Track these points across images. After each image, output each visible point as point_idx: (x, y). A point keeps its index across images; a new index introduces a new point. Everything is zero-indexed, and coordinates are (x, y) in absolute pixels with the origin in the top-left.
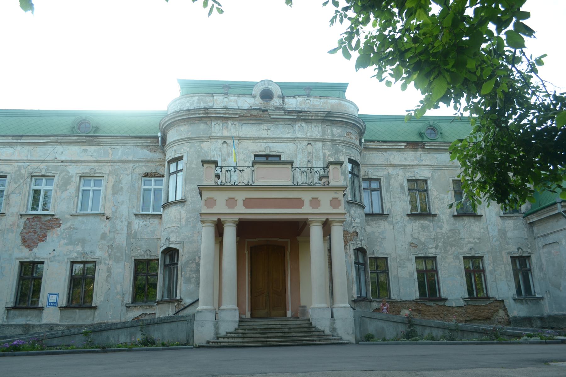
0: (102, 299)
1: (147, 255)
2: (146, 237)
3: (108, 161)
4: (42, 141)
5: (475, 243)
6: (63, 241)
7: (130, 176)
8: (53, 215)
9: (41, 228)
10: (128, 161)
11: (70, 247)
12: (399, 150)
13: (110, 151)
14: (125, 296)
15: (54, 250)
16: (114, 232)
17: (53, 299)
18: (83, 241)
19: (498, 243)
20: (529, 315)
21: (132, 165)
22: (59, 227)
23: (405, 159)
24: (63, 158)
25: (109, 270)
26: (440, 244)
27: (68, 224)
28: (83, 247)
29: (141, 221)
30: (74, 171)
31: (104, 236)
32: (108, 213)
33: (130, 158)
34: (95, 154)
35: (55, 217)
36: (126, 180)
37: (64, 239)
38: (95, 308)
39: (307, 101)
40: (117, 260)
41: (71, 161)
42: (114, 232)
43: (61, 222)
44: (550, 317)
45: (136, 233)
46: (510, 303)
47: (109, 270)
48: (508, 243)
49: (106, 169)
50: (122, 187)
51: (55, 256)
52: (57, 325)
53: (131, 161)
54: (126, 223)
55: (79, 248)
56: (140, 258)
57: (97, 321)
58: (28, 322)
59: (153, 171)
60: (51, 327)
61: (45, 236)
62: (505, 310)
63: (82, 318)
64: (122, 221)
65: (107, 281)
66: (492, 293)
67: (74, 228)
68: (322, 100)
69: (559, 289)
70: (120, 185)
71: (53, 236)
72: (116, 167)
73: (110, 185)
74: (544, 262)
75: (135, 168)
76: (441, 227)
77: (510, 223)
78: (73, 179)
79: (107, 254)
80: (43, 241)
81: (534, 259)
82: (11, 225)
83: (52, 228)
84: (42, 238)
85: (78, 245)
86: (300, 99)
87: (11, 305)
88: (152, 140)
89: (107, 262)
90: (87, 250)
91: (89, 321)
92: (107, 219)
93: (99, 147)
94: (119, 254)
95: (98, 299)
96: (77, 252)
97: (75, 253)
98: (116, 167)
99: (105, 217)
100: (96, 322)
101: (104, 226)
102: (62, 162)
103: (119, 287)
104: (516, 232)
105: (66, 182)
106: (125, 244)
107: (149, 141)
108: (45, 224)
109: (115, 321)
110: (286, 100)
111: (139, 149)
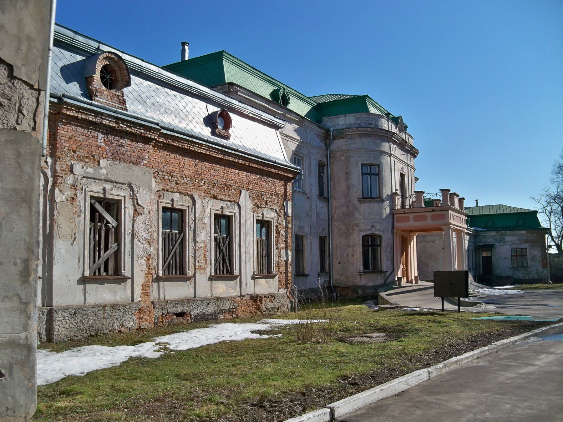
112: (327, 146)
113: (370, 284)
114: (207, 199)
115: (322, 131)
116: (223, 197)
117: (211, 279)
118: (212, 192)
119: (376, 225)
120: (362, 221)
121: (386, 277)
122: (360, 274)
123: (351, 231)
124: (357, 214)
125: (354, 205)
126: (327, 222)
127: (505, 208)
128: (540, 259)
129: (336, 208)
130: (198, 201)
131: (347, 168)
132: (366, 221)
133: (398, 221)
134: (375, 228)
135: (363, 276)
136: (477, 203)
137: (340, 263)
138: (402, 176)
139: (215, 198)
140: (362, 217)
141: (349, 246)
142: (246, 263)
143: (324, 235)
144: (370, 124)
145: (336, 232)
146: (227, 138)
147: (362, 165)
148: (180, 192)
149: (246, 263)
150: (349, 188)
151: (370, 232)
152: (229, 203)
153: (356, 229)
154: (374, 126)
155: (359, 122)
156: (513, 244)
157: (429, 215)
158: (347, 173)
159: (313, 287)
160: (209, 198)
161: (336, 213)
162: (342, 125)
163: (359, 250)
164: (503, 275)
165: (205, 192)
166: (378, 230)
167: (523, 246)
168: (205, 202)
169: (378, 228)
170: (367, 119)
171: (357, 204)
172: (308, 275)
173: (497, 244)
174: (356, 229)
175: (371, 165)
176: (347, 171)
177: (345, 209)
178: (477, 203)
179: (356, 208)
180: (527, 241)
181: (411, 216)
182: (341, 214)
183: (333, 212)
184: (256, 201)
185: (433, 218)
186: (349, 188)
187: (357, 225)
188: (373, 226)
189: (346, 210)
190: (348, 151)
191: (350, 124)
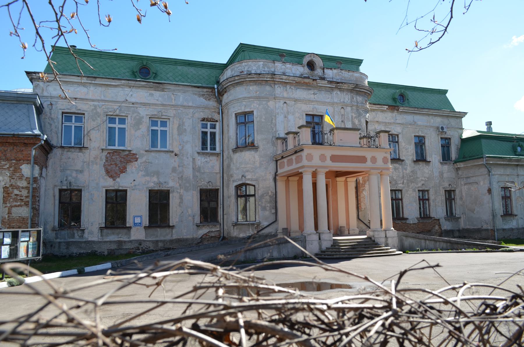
0: (177, 220)
1: (210, 186)
2: (207, 171)
3: (172, 105)
4: (114, 84)
5: (425, 181)
6: (141, 173)
7: (191, 120)
8: (130, 151)
9: (121, 161)
10: (189, 106)
11: (148, 178)
12: (382, 111)
13: (173, 97)
14: (195, 217)
15: (134, 180)
16: (182, 166)
17: (138, 220)
18: (157, 174)
19: (438, 181)
20: (452, 229)
21: (191, 110)
22: (136, 161)
23: (386, 118)
24: (133, 100)
25: (181, 198)
26: (405, 181)
27: (144, 159)
28: (158, 178)
30: (144, 112)
31: (174, 170)
32: (176, 151)
33: (190, 104)
34: (160, 99)
35: (132, 152)
36: (188, 124)
37: (142, 171)
38: (173, 227)
39: (340, 73)
40: (187, 190)
41: (141, 103)
42: (182, 166)
43: (137, 157)
44: (463, 229)
45: (199, 167)
46: (442, 221)
47: (181, 198)
48: (444, 181)
49: (171, 113)
50: (185, 129)
51: (135, 186)
52: (144, 241)
53: (191, 107)
54: (191, 159)
55: (155, 179)
56: (204, 188)
57: (175, 237)
58: (120, 239)
59: (210, 117)
60: (140, 242)
61: (125, 168)
62: (439, 225)
63: (162, 235)
64: (188, 158)
65: (180, 206)
66: (433, 215)
67: (149, 162)
68: (350, 74)
69: (473, 212)
70: (184, 127)
71: (131, 168)
72: (179, 111)
73: (176, 126)
74: (464, 194)
75: (194, 113)
76: (406, 169)
77: (446, 167)
78: (144, 120)
79: (178, 184)
80: (124, 172)
81: (457, 192)
82: (94, 158)
83: (131, 162)
84: (123, 170)
85: (153, 176)
86: (335, 71)
87: (103, 225)
88: (207, 90)
89: (179, 191)
90: (162, 180)
91: (168, 238)
92: (176, 155)
93: (163, 93)
94: (188, 185)
95: (173, 219)
96: (154, 182)
97: (153, 183)
98: (179, 111)
99: (174, 154)
101: (174, 162)
102: (133, 104)
103: (190, 210)
104: (449, 173)
105: (138, 122)
106: (191, 177)
107: (205, 90)
108: (124, 158)
109: (188, 237)
110: (326, 71)
111: (196, 96)
113: (242, 235)
119: (246, 174)
125: (230, 157)
132: (238, 171)
134: (245, 177)
135: (235, 227)
140: (234, 168)
147: (237, 115)
153: (231, 180)
154: (245, 73)
159: (185, 237)
166: (249, 179)
170: (240, 68)
175: (245, 114)
181: (285, 160)
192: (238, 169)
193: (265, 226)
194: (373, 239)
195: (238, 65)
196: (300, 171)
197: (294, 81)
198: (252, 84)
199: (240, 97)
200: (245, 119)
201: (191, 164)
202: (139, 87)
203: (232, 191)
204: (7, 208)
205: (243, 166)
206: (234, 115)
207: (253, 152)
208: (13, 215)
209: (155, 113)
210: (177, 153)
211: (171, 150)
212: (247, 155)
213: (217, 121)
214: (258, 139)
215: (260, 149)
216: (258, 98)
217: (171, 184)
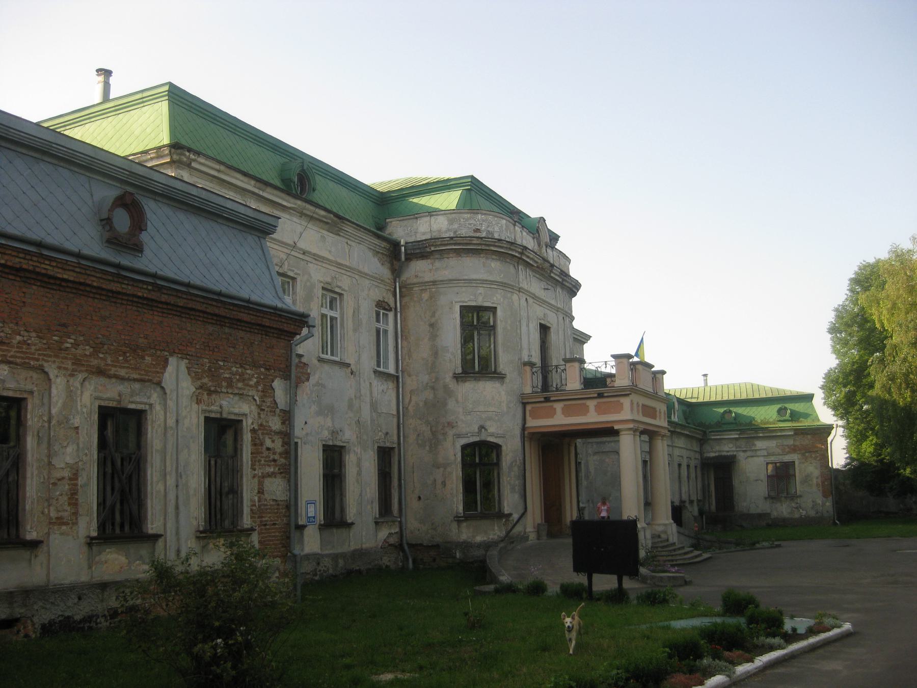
4: (285, 203)
21: (367, 282)
22: (308, 380)
29: (380, 383)
33: (366, 270)
52: (323, 556)
55: (329, 423)
60: (316, 558)
73: (351, 312)
93: (337, 237)
100: (352, 549)
102: (304, 253)
112: (396, 273)
113: (479, 539)
114: (80, 377)
115: (384, 244)
116: (122, 373)
117: (91, 542)
118: (95, 362)
120: (463, 417)
121: (510, 525)
122: (459, 520)
123: (441, 437)
124: (451, 404)
125: (446, 387)
126: (395, 420)
127: (725, 389)
128: (819, 481)
129: (412, 392)
130: (59, 380)
131: (433, 315)
133: (534, 416)
134: (486, 430)
135: (465, 524)
136: (706, 381)
137: (420, 498)
138: (544, 329)
139: (100, 372)
140: (461, 410)
141: (437, 466)
142: (177, 508)
143: (388, 445)
144: (477, 230)
145: (412, 438)
146: (137, 248)
148: (9, 363)
149: (177, 508)
150: (435, 354)
151: (476, 439)
152: (137, 386)
153: (451, 433)
154: (484, 235)
155: (456, 226)
156: (769, 455)
157: (592, 404)
158: (432, 325)
159: (364, 546)
160: (85, 375)
161: (413, 403)
162: (424, 234)
163: (456, 474)
164: (753, 511)
165: (77, 362)
166: (492, 435)
167: (787, 458)
168: (76, 382)
169: (491, 430)
171: (452, 385)
172: (352, 524)
173: (742, 454)
174: (451, 433)
175: (479, 309)
176: (433, 320)
177: (428, 395)
178: (706, 381)
179: (449, 392)
180: (794, 449)
181: (558, 406)
182: (421, 404)
183: (407, 400)
184: (206, 380)
185: (599, 410)
186: (435, 354)
187: (451, 425)
188: (482, 427)
189: (431, 396)
190: (434, 283)
191: (439, 231)
192: (469, 413)
193: (515, 520)
194: (663, 536)
195: (469, 216)
196: (616, 427)
197: (537, 262)
198: (494, 257)
199: (474, 277)
200: (477, 322)
201: (368, 393)
202: (311, 218)
203: (452, 452)
204: (256, 480)
205: (481, 408)
206: (457, 309)
207: (497, 384)
208: (266, 496)
209: (329, 280)
210: (354, 370)
211: (347, 361)
212: (487, 389)
213: (390, 310)
214: (505, 361)
215: (507, 380)
216: (504, 285)
217: (348, 435)
